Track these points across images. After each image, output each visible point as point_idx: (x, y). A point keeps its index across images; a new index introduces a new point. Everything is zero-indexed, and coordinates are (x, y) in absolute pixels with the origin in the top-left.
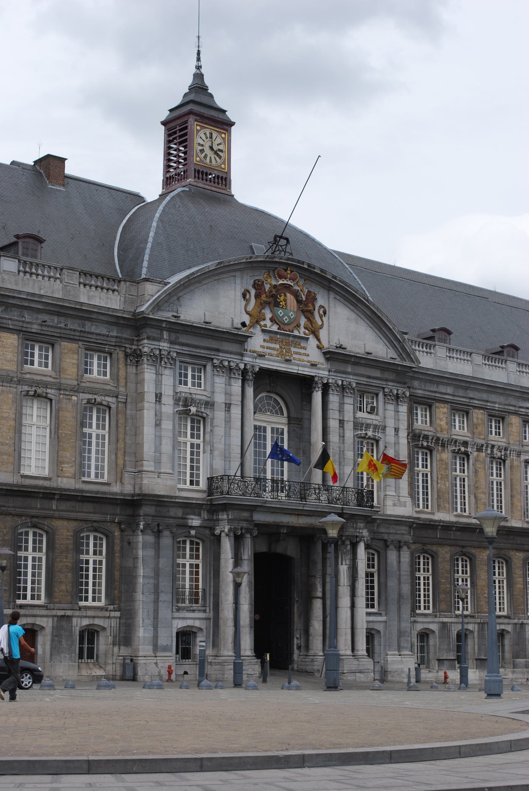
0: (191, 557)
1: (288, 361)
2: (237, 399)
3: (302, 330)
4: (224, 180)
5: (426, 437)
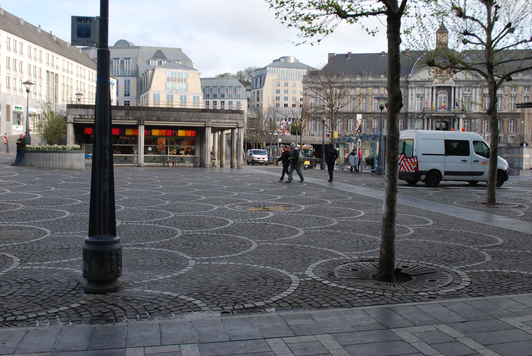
4: (447, 44)
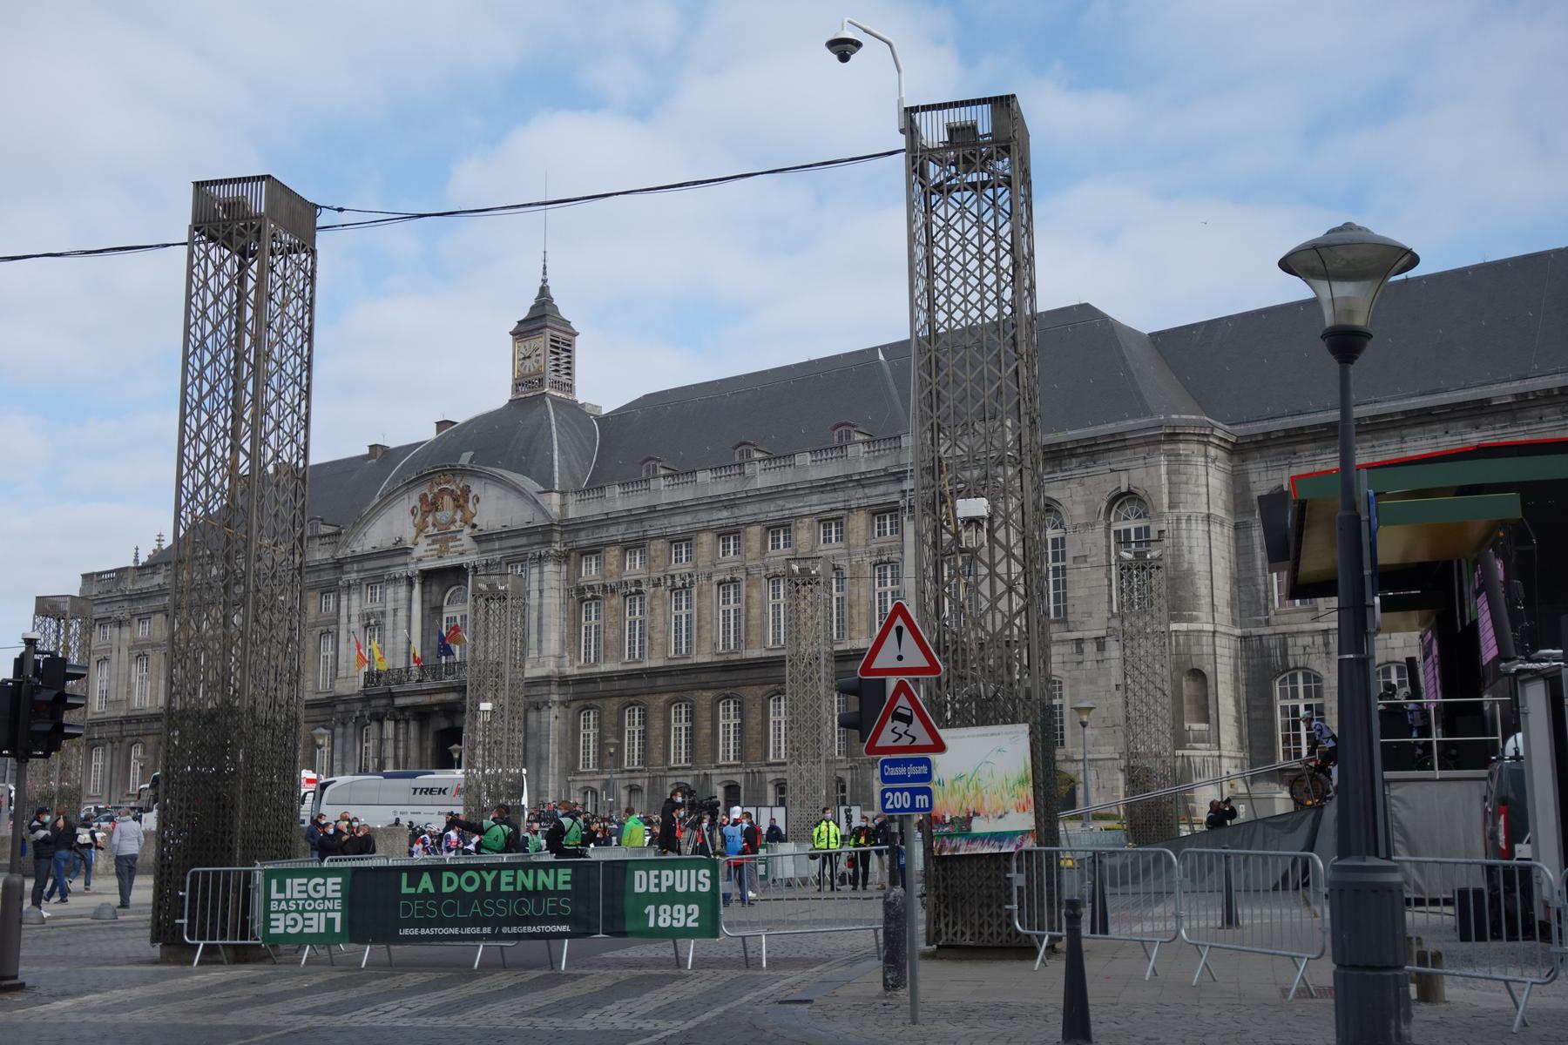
5: (591, 588)
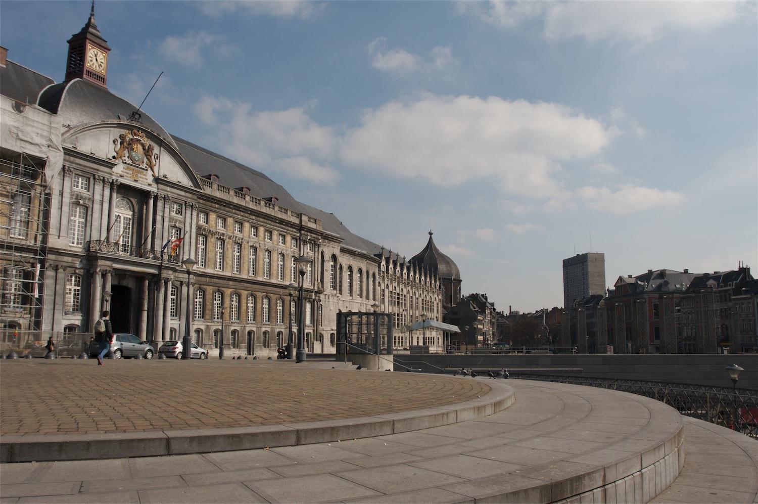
0: (75, 285)
1: (136, 181)
2: (107, 198)
3: (145, 165)
5: (204, 230)
